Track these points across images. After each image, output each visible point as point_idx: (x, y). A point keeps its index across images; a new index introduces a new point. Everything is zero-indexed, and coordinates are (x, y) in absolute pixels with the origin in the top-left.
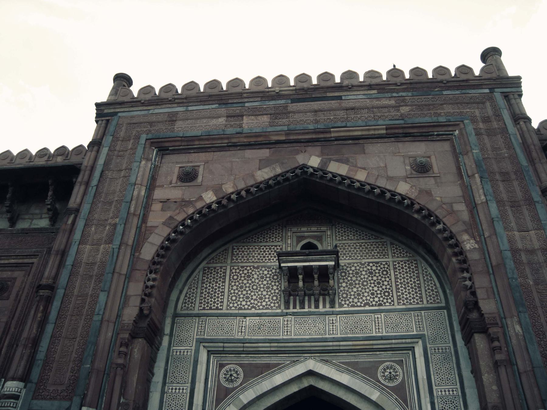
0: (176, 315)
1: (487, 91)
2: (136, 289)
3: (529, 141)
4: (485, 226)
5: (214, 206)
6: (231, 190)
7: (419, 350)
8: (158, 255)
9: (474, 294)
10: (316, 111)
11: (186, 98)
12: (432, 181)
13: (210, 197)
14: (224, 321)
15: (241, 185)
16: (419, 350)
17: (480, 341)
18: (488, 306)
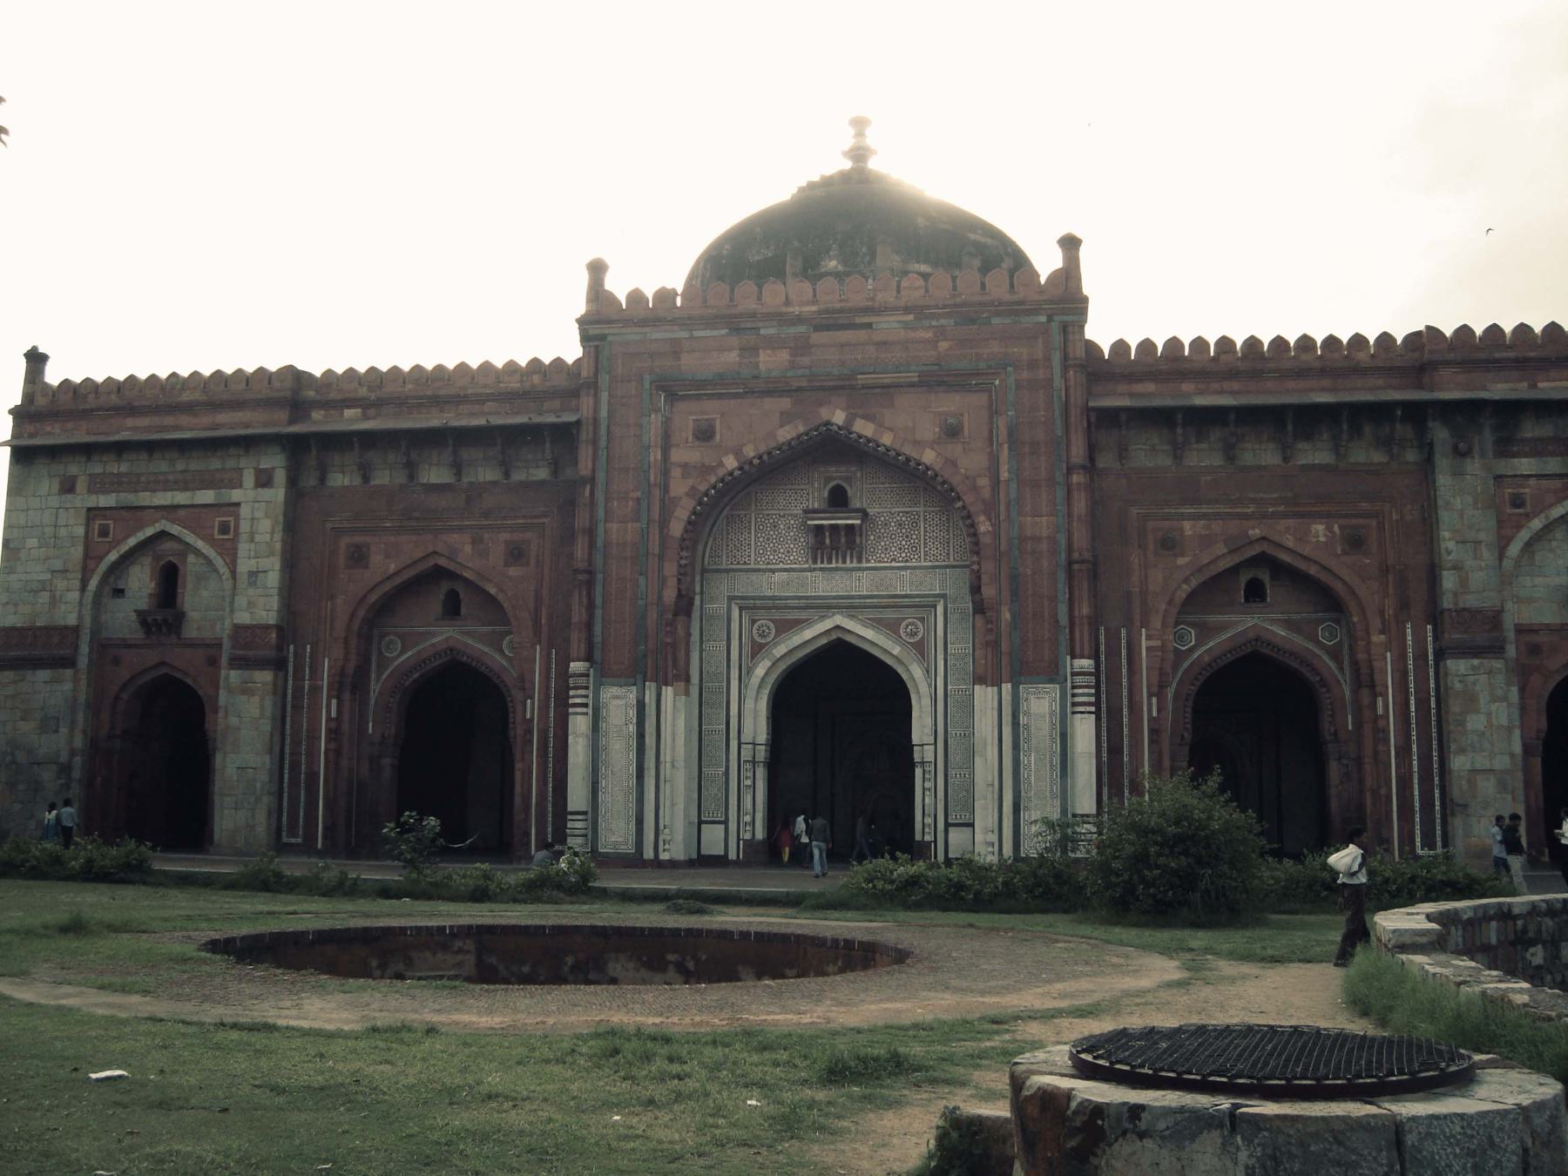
0: (704, 571)
1: (1043, 319)
2: (670, 569)
3: (1072, 400)
4: (1002, 508)
5: (737, 473)
6: (752, 454)
7: (940, 609)
8: (686, 531)
9: (979, 578)
10: (842, 345)
11: (689, 318)
12: (959, 447)
13: (731, 463)
14: (754, 577)
15: (763, 449)
16: (940, 609)
17: (980, 620)
18: (988, 591)
